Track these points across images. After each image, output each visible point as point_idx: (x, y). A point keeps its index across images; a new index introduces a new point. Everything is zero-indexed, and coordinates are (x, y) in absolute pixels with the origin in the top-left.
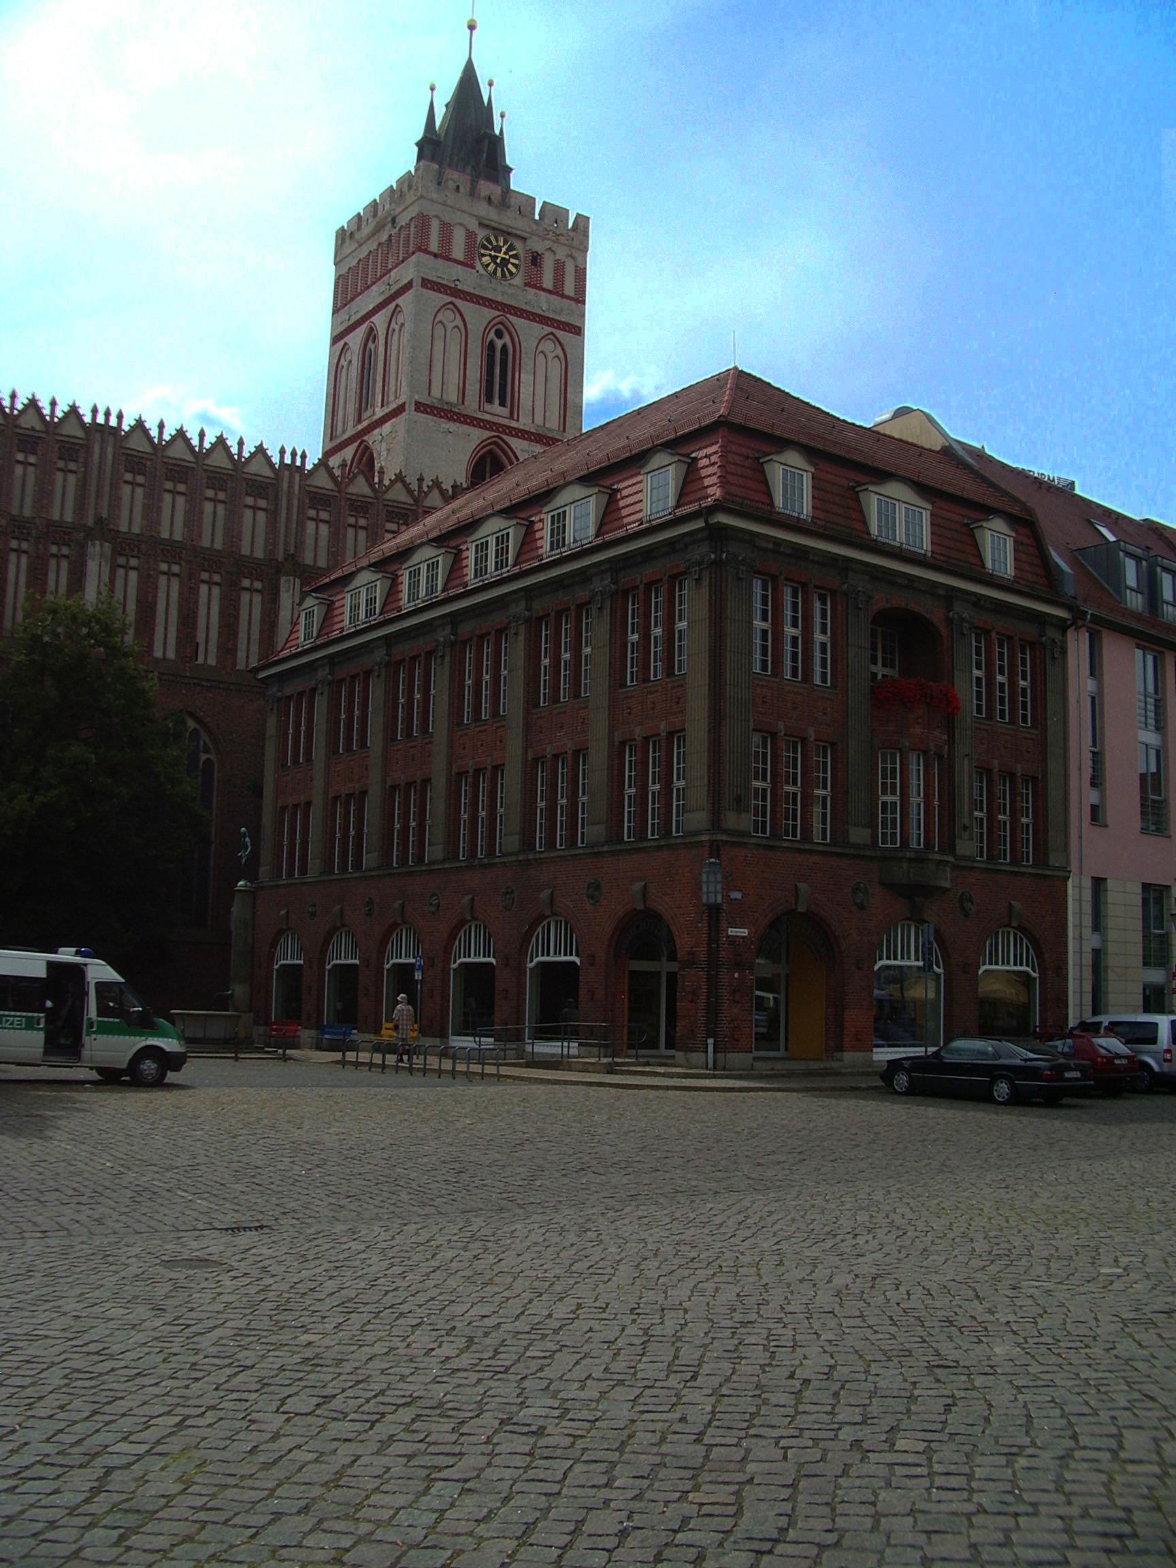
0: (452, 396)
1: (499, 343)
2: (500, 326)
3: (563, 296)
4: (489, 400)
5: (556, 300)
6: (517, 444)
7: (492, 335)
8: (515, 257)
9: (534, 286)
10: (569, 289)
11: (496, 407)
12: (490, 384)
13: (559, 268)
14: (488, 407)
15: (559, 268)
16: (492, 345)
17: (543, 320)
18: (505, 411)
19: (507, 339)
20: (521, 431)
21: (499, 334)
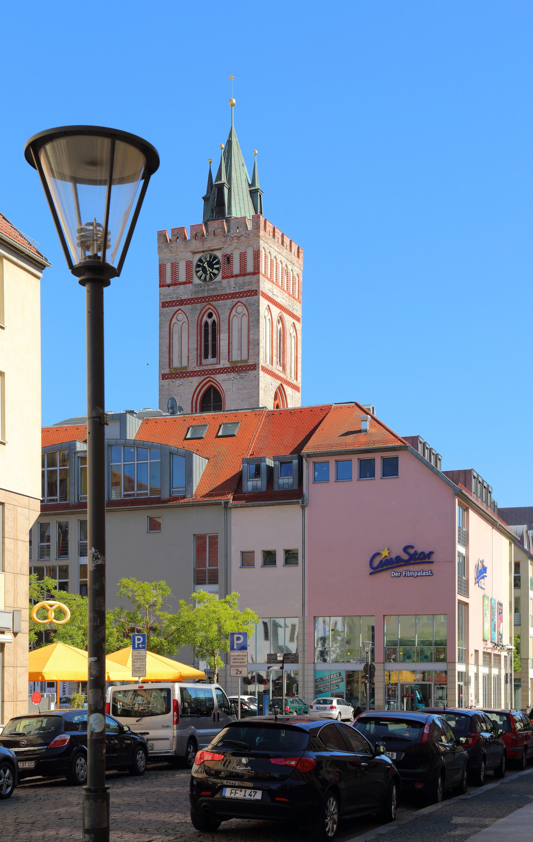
0: (185, 364)
1: (210, 321)
2: (210, 311)
3: (245, 275)
4: (206, 357)
5: (240, 279)
6: (219, 378)
7: (205, 318)
8: (218, 263)
9: (227, 277)
10: (250, 268)
11: (210, 360)
12: (206, 347)
13: (243, 257)
14: (204, 361)
15: (243, 257)
16: (206, 323)
17: (233, 296)
18: (213, 360)
19: (214, 317)
20: (221, 369)
21: (210, 315)
